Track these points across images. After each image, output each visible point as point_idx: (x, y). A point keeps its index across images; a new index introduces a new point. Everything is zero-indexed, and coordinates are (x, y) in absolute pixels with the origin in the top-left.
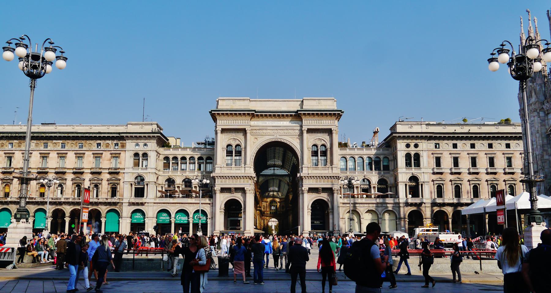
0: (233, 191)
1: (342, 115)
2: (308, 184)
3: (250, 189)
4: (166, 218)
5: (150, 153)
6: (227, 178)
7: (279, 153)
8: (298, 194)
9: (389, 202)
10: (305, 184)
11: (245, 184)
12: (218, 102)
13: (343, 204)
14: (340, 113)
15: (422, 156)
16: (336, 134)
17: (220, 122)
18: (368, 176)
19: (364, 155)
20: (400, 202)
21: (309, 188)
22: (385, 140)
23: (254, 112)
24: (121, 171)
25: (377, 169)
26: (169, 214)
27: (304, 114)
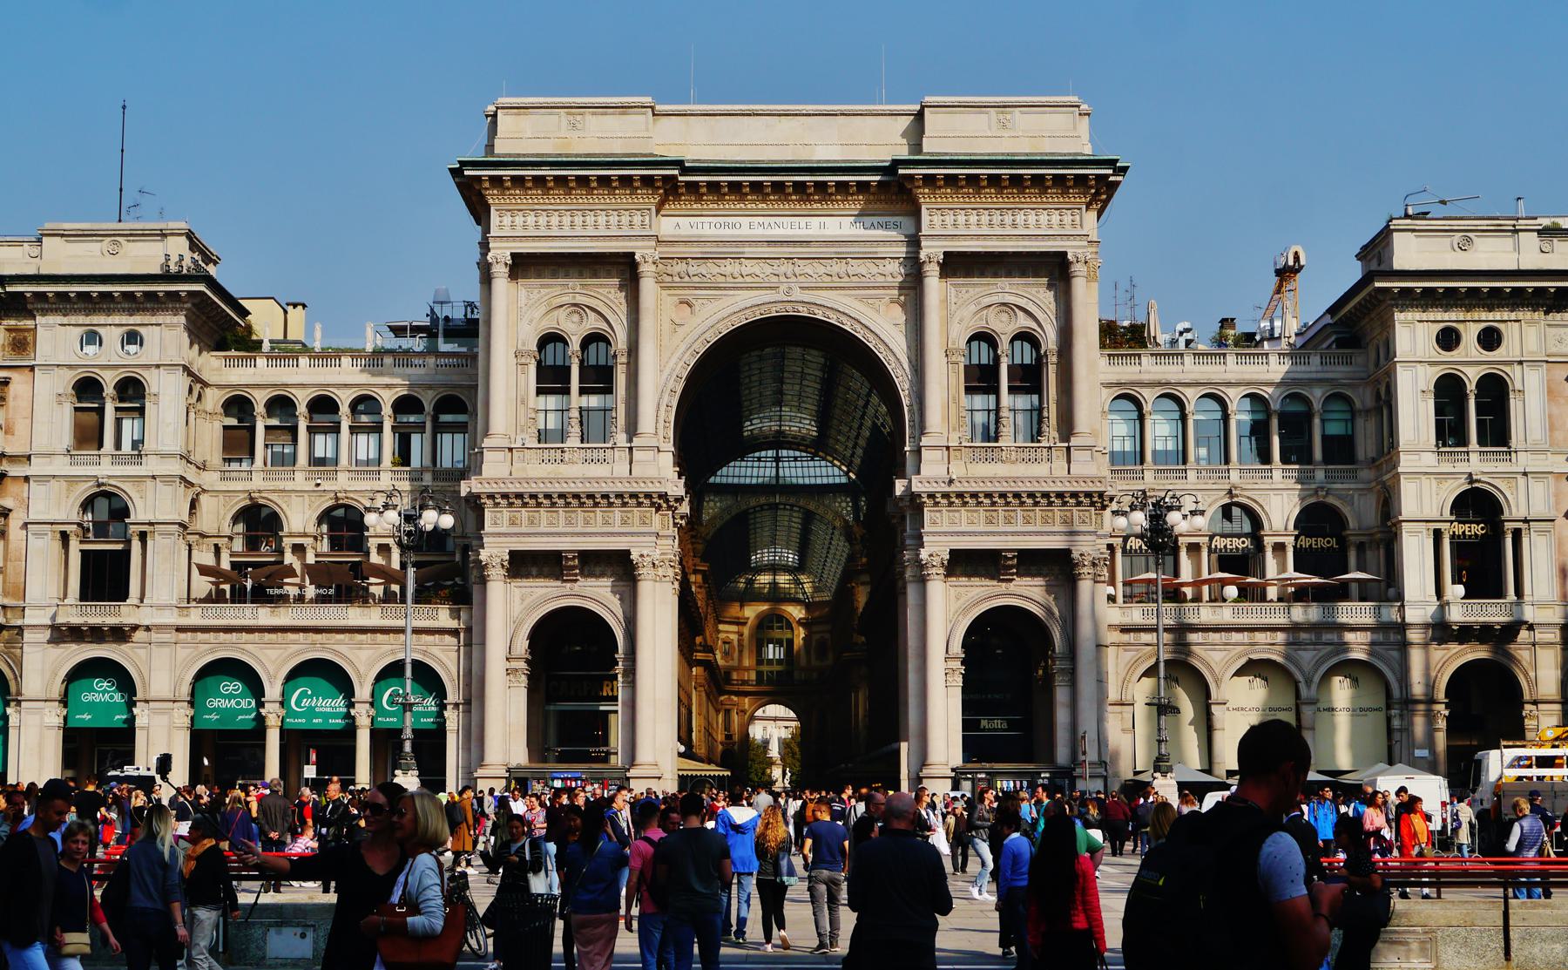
0: (574, 568)
1: (1117, 184)
2: (945, 534)
3: (657, 555)
4: (238, 703)
5: (154, 382)
6: (539, 505)
7: (802, 379)
8: (900, 583)
9: (1351, 621)
10: (934, 534)
11: (632, 534)
12: (494, 123)
13: (1125, 630)
14: (1107, 176)
15: (1521, 389)
16: (1089, 279)
17: (507, 220)
18: (1246, 493)
19: (1229, 384)
20: (1408, 619)
21: (952, 552)
22: (1332, 310)
23: (676, 172)
24: (14, 470)
25: (1293, 458)
26: (254, 684)
27: (930, 180)
